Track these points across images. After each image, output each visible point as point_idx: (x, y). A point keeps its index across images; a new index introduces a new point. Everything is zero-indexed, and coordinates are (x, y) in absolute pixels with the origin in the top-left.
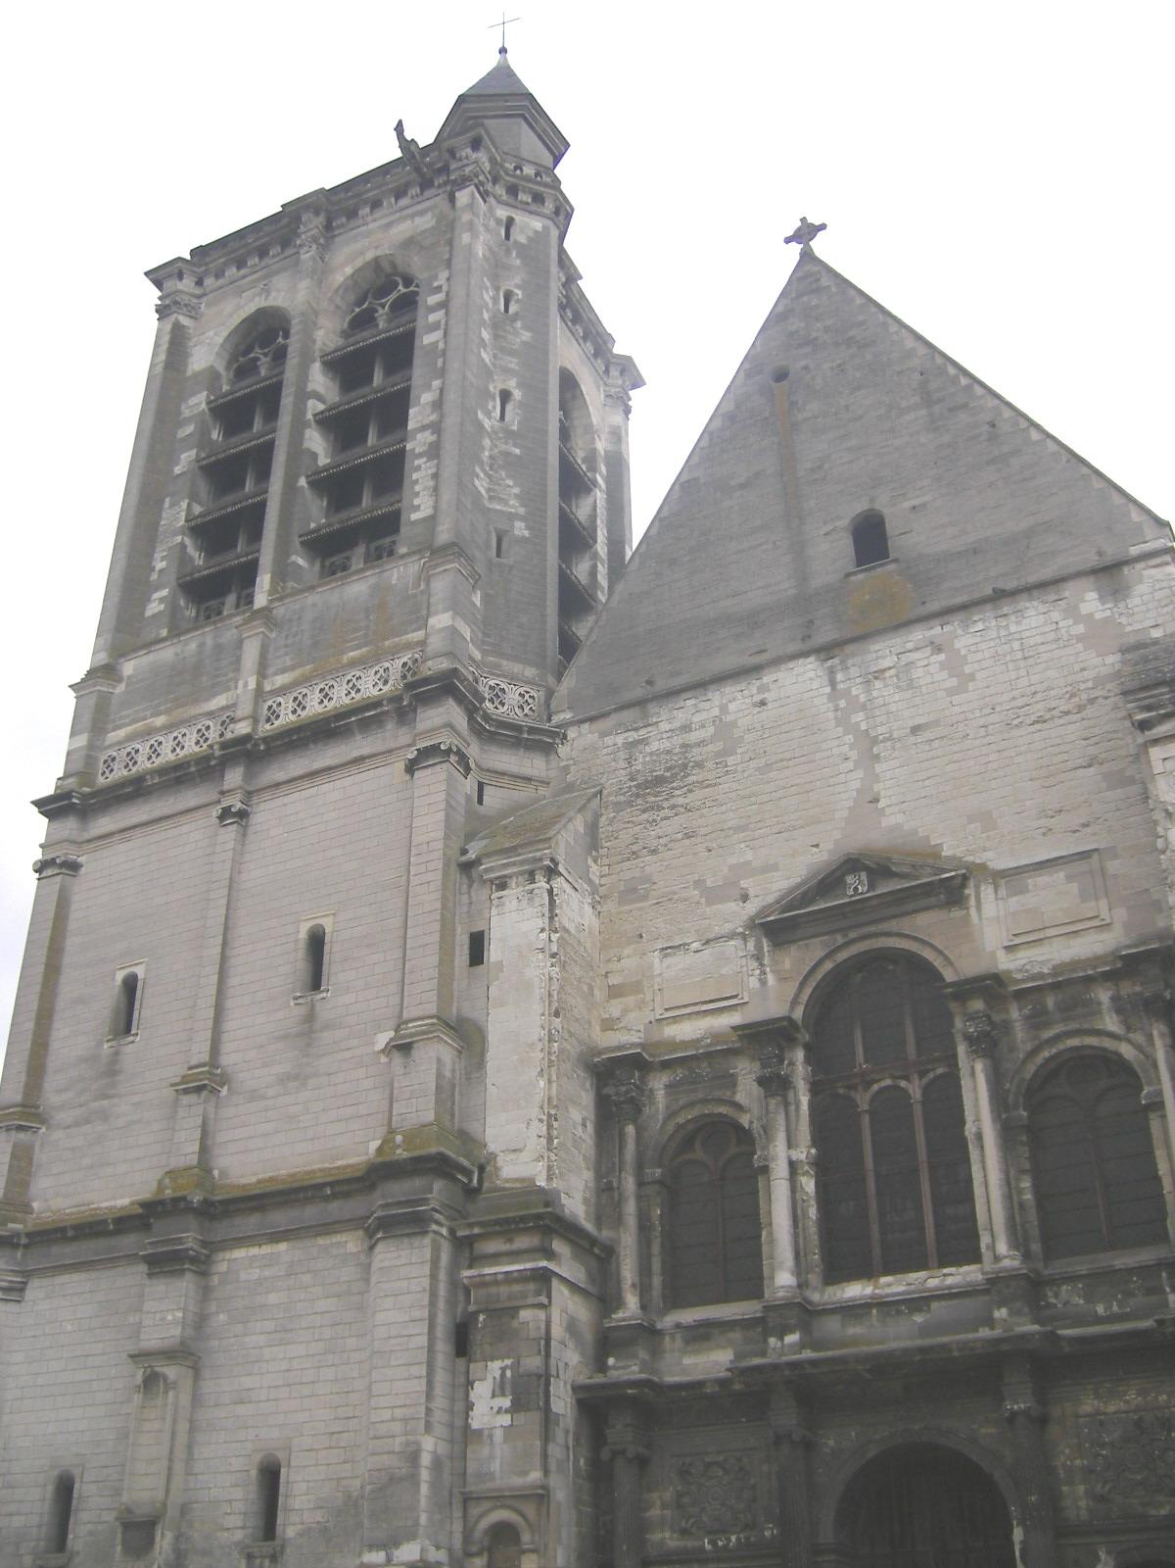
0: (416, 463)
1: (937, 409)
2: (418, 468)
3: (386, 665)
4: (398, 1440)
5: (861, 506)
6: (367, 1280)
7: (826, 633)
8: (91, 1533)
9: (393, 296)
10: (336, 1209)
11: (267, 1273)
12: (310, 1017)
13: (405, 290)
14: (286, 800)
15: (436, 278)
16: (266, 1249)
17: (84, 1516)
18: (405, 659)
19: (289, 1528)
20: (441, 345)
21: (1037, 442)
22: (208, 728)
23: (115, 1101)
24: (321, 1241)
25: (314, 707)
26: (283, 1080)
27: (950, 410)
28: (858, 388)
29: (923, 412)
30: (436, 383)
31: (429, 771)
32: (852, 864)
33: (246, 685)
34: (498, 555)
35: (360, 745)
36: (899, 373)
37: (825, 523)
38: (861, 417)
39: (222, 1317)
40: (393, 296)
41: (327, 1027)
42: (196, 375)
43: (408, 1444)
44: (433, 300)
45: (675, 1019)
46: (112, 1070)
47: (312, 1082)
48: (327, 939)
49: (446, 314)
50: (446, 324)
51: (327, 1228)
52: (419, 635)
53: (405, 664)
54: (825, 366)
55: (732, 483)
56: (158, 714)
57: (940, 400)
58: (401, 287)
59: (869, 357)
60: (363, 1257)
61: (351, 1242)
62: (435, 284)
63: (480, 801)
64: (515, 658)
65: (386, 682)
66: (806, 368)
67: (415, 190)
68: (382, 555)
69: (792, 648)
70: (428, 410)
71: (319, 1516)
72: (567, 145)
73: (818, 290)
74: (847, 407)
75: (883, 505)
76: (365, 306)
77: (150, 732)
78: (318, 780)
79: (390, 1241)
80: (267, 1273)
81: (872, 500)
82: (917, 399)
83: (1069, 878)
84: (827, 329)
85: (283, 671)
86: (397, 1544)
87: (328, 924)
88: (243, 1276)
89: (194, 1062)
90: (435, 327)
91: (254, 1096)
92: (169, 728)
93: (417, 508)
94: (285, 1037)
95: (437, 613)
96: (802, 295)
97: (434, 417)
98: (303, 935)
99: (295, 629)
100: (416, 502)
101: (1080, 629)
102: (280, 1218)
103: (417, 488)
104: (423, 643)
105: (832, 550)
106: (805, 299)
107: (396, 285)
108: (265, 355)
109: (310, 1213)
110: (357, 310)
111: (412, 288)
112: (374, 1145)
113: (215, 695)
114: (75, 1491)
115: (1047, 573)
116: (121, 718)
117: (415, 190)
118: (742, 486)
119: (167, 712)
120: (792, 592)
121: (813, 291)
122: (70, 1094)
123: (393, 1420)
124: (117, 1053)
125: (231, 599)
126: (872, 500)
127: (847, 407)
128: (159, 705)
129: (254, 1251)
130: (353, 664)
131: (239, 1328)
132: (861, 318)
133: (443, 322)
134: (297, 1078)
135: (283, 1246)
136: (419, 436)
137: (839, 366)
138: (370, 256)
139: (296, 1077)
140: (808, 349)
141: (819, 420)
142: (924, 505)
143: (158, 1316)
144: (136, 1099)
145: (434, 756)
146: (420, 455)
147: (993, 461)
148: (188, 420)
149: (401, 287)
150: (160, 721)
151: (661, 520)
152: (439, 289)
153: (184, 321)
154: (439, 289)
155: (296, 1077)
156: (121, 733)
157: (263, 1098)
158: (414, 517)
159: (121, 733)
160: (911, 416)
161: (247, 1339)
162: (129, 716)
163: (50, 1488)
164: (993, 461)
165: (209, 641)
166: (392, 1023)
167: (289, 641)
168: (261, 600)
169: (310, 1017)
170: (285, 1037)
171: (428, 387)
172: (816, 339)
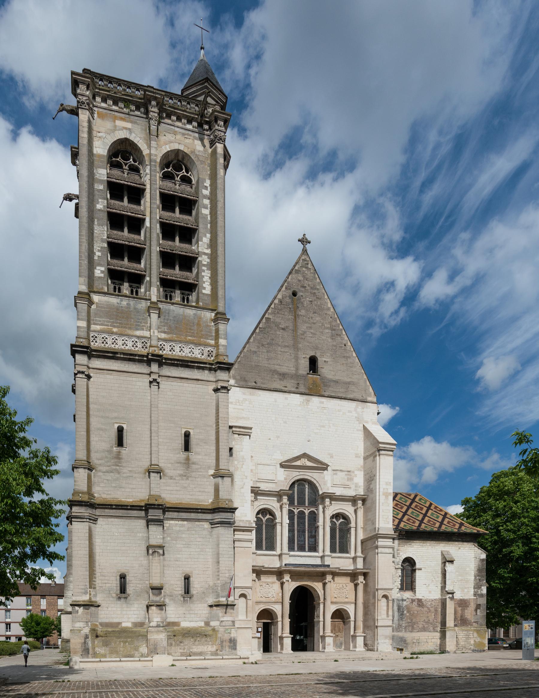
1: (333, 332)
5: (312, 354)
7: (302, 389)
27: (337, 335)
29: (330, 331)
37: (304, 354)
38: (314, 323)
54: (307, 299)
55: (280, 326)
57: (334, 330)
59: (319, 303)
66: (302, 296)
73: (307, 268)
75: (318, 355)
82: (329, 326)
84: (309, 285)
105: (305, 364)
106: (304, 269)
118: (283, 329)
120: (294, 372)
126: (315, 353)
132: (318, 287)
137: (311, 301)
140: (303, 289)
141: (305, 318)
142: (328, 362)
147: (344, 357)
151: (260, 328)
160: (327, 331)
164: (344, 357)
172: (306, 287)
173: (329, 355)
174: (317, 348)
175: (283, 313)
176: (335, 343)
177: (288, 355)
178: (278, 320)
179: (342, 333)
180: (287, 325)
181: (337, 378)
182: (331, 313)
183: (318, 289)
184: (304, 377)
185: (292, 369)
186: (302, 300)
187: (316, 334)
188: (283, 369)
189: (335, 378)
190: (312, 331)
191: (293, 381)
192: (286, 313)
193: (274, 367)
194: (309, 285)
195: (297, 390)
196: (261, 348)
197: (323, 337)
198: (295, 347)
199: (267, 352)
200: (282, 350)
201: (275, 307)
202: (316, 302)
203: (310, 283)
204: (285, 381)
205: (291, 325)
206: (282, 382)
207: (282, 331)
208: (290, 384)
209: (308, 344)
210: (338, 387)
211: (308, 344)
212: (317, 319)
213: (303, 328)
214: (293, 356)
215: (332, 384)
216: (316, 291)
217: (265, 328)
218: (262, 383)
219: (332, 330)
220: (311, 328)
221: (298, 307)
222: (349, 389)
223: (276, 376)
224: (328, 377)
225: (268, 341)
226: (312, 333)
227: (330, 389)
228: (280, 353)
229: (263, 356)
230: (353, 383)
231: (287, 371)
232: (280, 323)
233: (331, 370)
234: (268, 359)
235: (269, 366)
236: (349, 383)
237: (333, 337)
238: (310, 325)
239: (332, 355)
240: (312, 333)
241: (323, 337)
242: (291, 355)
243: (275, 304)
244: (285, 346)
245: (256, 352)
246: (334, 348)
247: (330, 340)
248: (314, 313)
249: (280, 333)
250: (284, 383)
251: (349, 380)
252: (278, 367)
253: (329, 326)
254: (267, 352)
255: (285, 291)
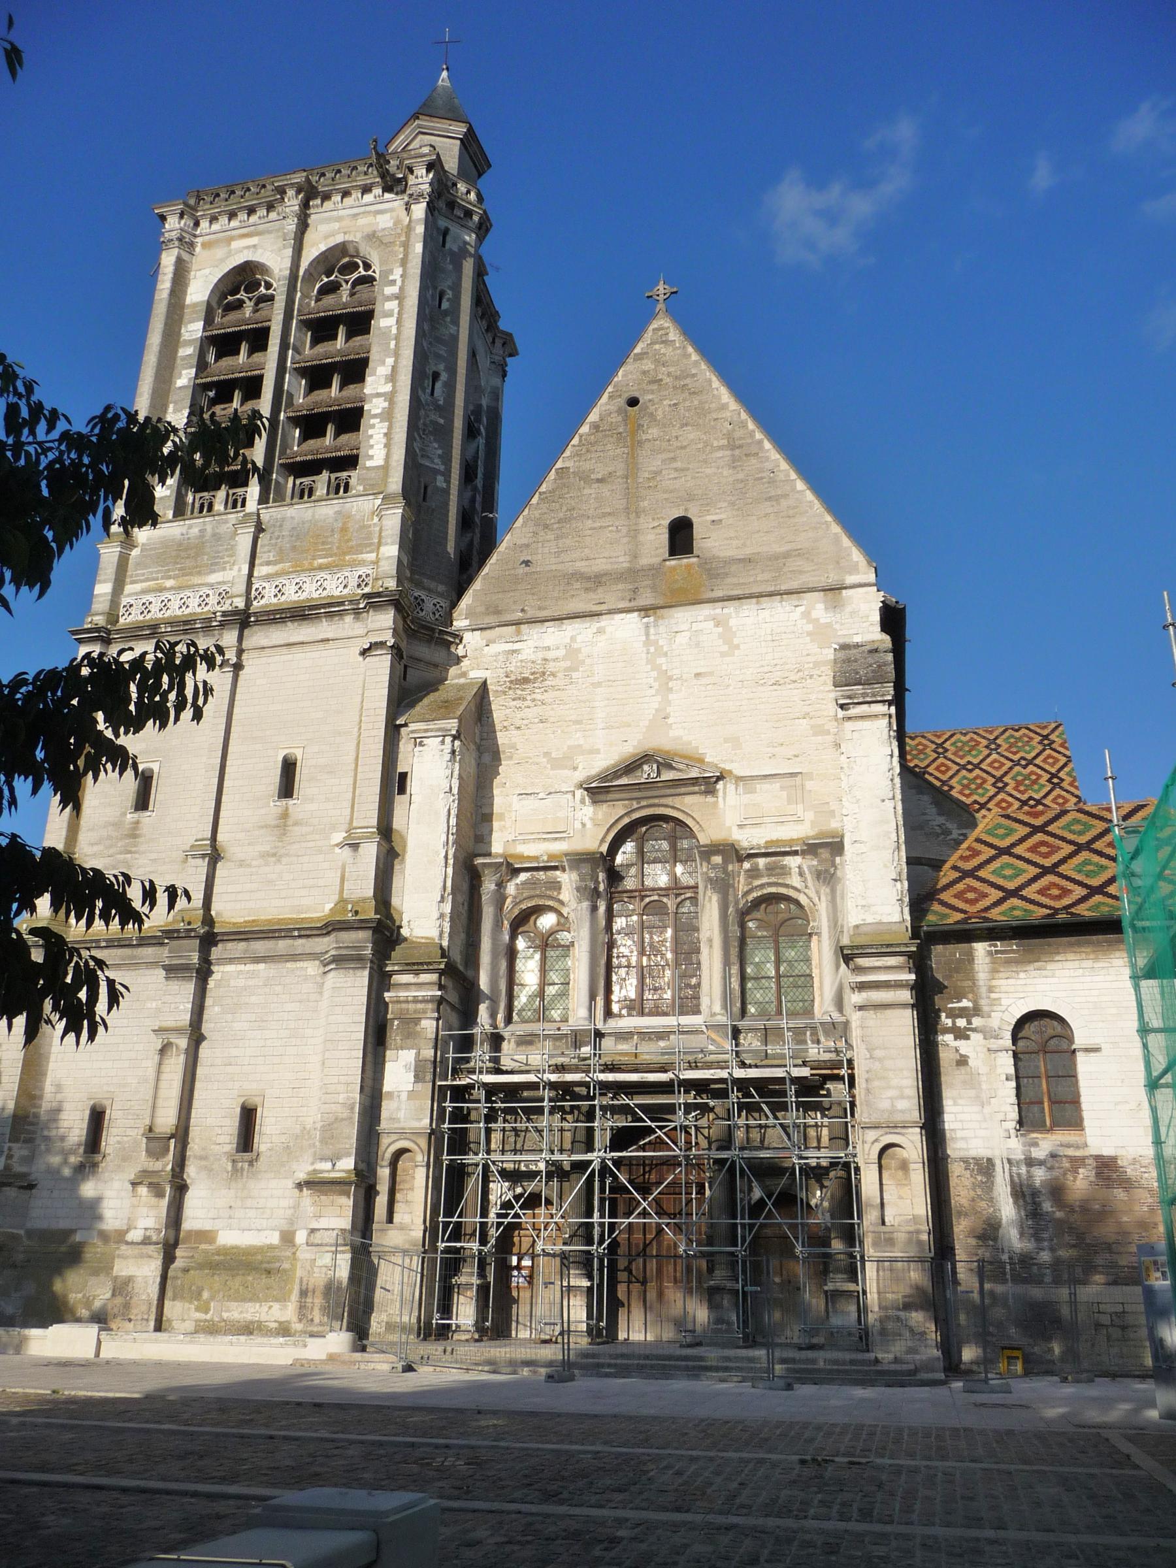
0: (372, 421)
1: (737, 452)
2: (373, 426)
3: (347, 574)
4: (342, 1096)
6: (321, 993)
7: (646, 599)
8: (119, 1142)
9: (355, 276)
10: (301, 945)
11: (251, 982)
12: (285, 815)
13: (363, 273)
14: (270, 660)
15: (391, 271)
16: (250, 967)
17: (113, 1131)
18: (360, 573)
19: (262, 1142)
20: (394, 331)
21: (799, 492)
22: (208, 596)
23: (137, 856)
24: (289, 965)
25: (291, 596)
26: (264, 855)
28: (686, 425)
29: (728, 453)
30: (390, 361)
31: (377, 658)
32: (645, 758)
33: (240, 570)
34: (424, 499)
35: (324, 629)
36: (715, 420)
37: (653, 519)
39: (217, 1009)
40: (355, 276)
41: (296, 824)
42: (195, 305)
43: (348, 1099)
44: (389, 290)
45: (524, 841)
46: (134, 833)
47: (284, 860)
48: (298, 764)
49: (400, 305)
50: (399, 313)
51: (294, 957)
52: (372, 556)
53: (360, 577)
55: (593, 476)
56: (169, 578)
57: (740, 447)
58: (361, 269)
59: (696, 403)
60: (319, 979)
61: (312, 968)
62: (391, 278)
63: (405, 678)
64: (432, 578)
65: (345, 586)
67: (378, 191)
68: (340, 489)
69: (621, 605)
70: (383, 381)
71: (283, 1139)
72: (490, 166)
73: (665, 342)
74: (677, 437)
76: (332, 278)
77: (161, 589)
78: (294, 649)
79: (341, 971)
80: (251, 982)
81: (686, 510)
82: (725, 442)
83: (782, 788)
84: (669, 374)
85: (268, 563)
86: (339, 1158)
87: (298, 754)
88: (232, 983)
89: (200, 837)
90: (389, 314)
91: (242, 863)
92: (180, 588)
93: (371, 458)
94: (266, 826)
95: (387, 544)
96: (656, 343)
97: (388, 388)
98: (280, 759)
99: (276, 534)
100: (371, 452)
101: (810, 627)
102: (260, 947)
103: (372, 442)
104: (376, 562)
105: (657, 539)
106: (657, 347)
107: (357, 267)
108: (250, 299)
109: (282, 945)
110: (326, 280)
111: (370, 273)
112: (330, 906)
113: (214, 571)
114: (107, 1117)
115: (794, 585)
116: (137, 575)
117: (378, 191)
118: (599, 481)
119: (175, 577)
120: (626, 565)
121: (663, 342)
122: (101, 847)
123: (339, 1083)
124: (138, 822)
125: (221, 494)
126: (686, 510)
127: (677, 437)
128: (169, 570)
129: (241, 967)
130: (321, 568)
131: (229, 1017)
132: (694, 371)
133: (396, 311)
134: (274, 856)
135: (262, 966)
136: (374, 400)
137: (675, 405)
138: (339, 239)
139: (274, 855)
140: (655, 387)
143: (173, 1006)
144: (154, 856)
145: (382, 649)
146: (375, 416)
147: (770, 499)
148: (189, 343)
149: (361, 269)
150: (169, 583)
152: (393, 282)
153: (185, 256)
154: (393, 282)
155: (274, 855)
156: (138, 587)
157: (249, 866)
158: (369, 464)
159: (138, 587)
160: (720, 454)
161: (235, 1025)
162: (143, 574)
163: (88, 1112)
165: (209, 528)
166: (346, 827)
167: (273, 541)
168: (252, 505)
169: (285, 815)
170: (266, 826)
171: (383, 363)
172: (661, 380)
173: (724, 505)
174: (691, 498)
175: (599, 448)
176: (741, 476)
177: (611, 531)
178: (587, 466)
179: (761, 448)
180: (610, 469)
181: (748, 551)
182: (729, 414)
183: (694, 375)
184: (655, 571)
185: (621, 559)
186: (652, 409)
187: (688, 469)
188: (600, 565)
189: (740, 554)
190: (678, 464)
191: (620, 586)
192: (609, 447)
193: (569, 568)
194: (669, 374)
195: (633, 604)
196: (542, 533)
197: (708, 471)
198: (632, 509)
199: (557, 538)
200: (598, 524)
201: (580, 441)
202: (687, 404)
203: (672, 369)
204: (600, 590)
205: (620, 468)
206: (592, 595)
207: (596, 485)
208: (612, 596)
209: (666, 496)
210: (752, 572)
211: (666, 496)
212: (691, 436)
213: (650, 463)
214: (624, 530)
215: (734, 568)
216: (688, 381)
217: (553, 491)
218: (540, 608)
219: (732, 450)
220: (674, 459)
221: (640, 426)
222: (785, 569)
223: (577, 585)
224: (722, 554)
225: (561, 515)
226: (676, 470)
227: (729, 580)
228: (589, 532)
229: (546, 550)
230: (799, 553)
231: (609, 567)
232: (592, 471)
233: (731, 538)
234: (558, 554)
235: (560, 567)
236: (787, 555)
237: (734, 463)
238: (672, 455)
239: (733, 504)
240: (676, 470)
241: (708, 471)
242: (618, 531)
243: (581, 436)
244: (605, 515)
245: (527, 546)
246: (741, 485)
247: (725, 473)
248: (683, 425)
249: (592, 491)
250: (600, 594)
251: (783, 549)
252: (584, 563)
253: (725, 442)
254: (557, 538)
255: (606, 404)
